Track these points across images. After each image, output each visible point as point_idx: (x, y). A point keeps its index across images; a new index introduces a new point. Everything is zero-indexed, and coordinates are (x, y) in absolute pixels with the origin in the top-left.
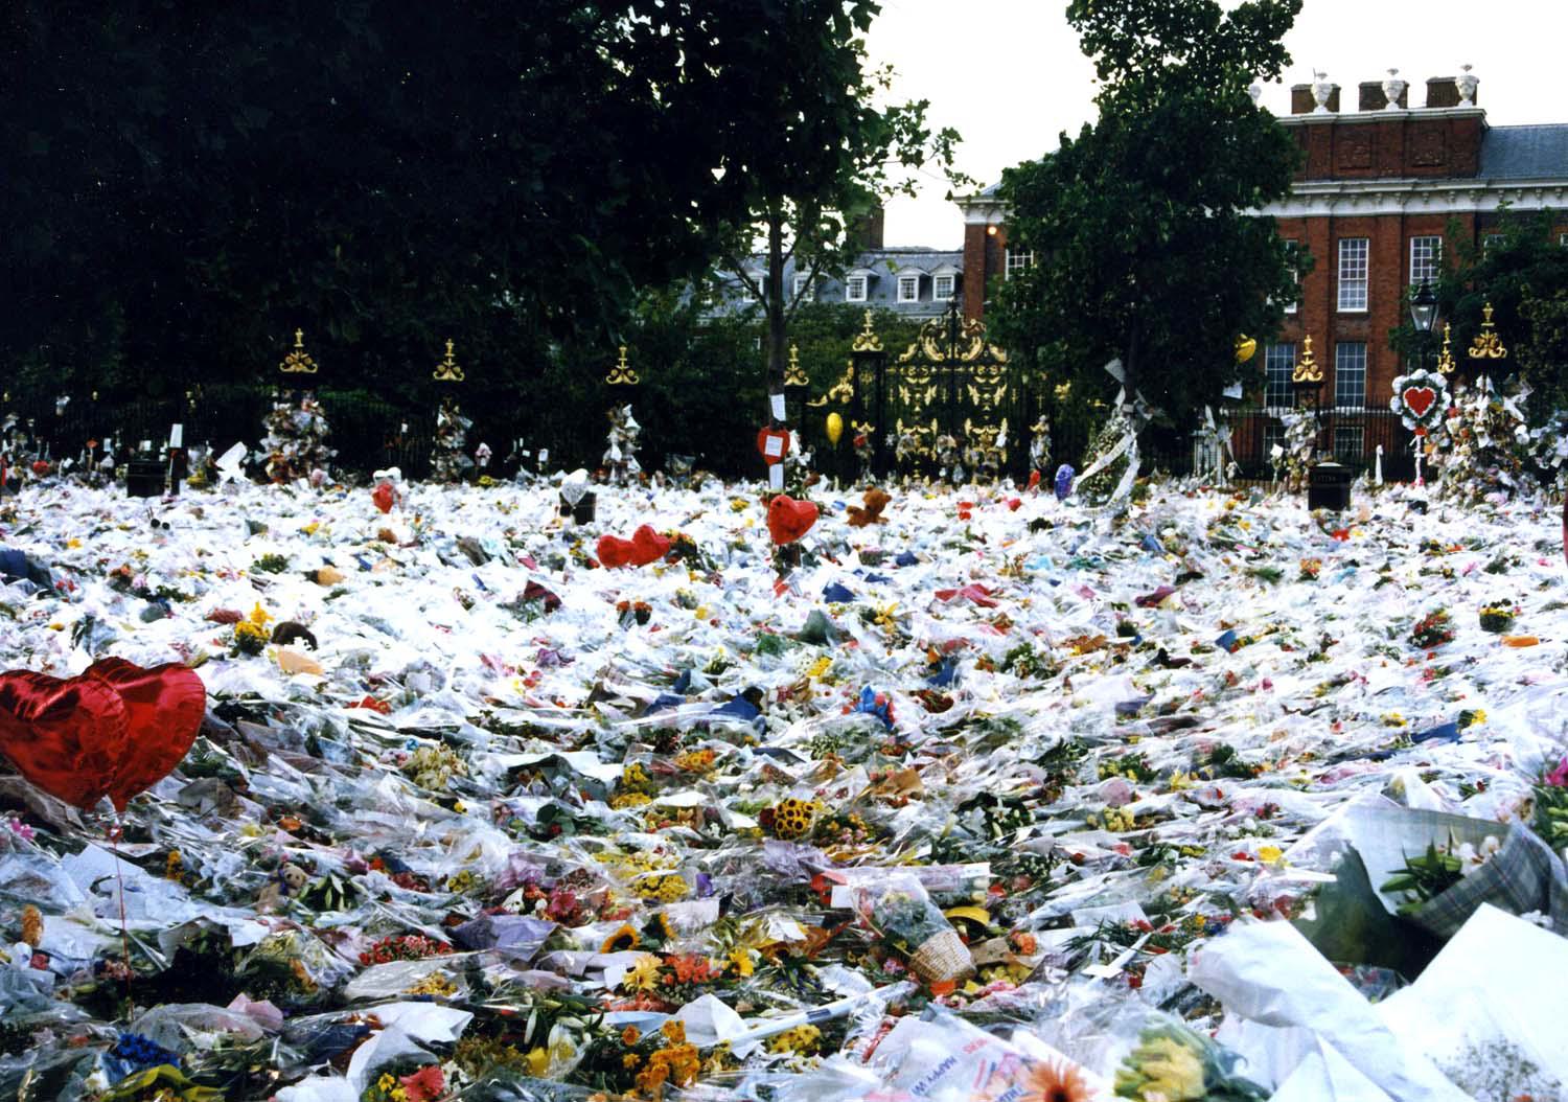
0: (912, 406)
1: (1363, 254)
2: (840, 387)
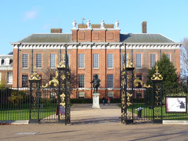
2: (53, 81)
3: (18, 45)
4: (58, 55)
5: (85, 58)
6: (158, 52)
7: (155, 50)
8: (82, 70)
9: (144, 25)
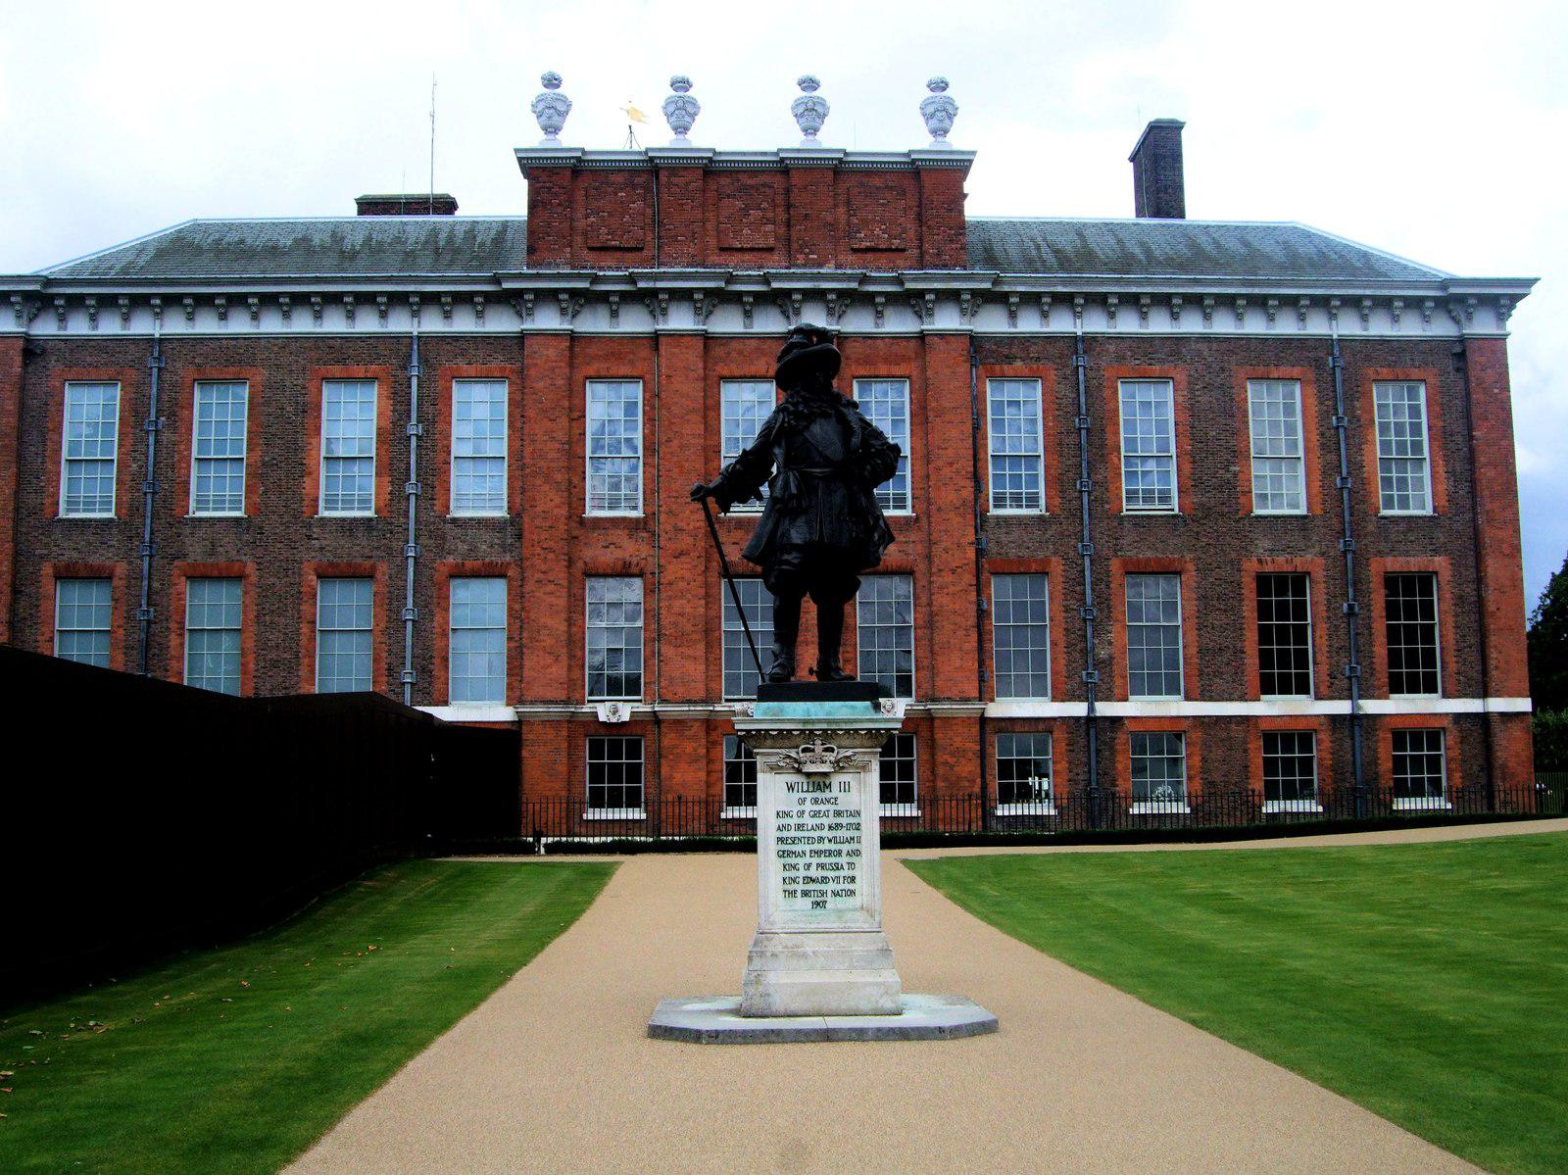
3: (28, 296)
4: (398, 398)
5: (649, 420)
6: (1319, 364)
7: (1287, 342)
8: (620, 535)
9: (1158, 160)
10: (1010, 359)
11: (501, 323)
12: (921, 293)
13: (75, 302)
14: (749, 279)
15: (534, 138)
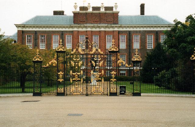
0: (75, 67)
1: (97, 38)
2: (52, 61)
7: (152, 31)
10: (122, 33)
11: (71, 29)
12: (113, 27)
13: (27, 27)
14: (96, 25)
15: (74, 10)
